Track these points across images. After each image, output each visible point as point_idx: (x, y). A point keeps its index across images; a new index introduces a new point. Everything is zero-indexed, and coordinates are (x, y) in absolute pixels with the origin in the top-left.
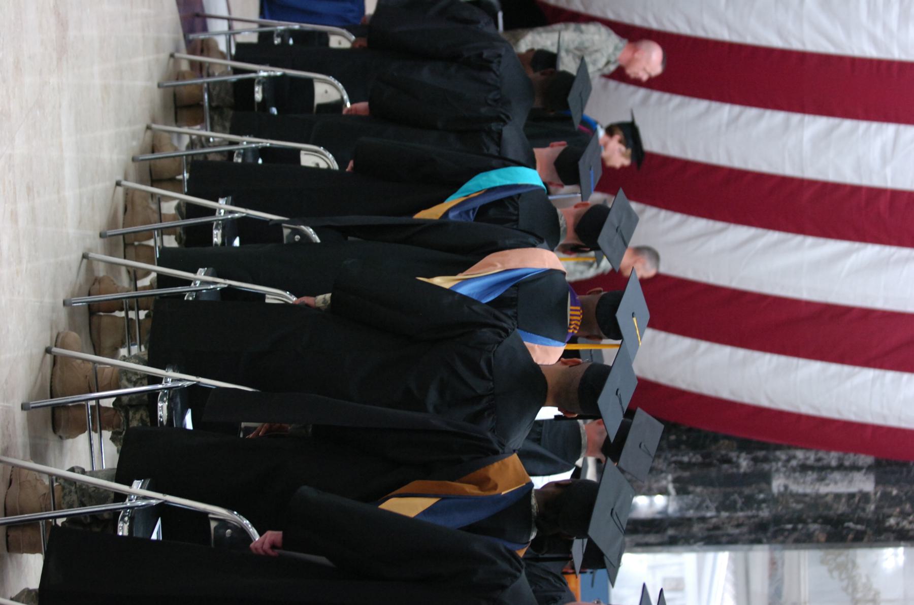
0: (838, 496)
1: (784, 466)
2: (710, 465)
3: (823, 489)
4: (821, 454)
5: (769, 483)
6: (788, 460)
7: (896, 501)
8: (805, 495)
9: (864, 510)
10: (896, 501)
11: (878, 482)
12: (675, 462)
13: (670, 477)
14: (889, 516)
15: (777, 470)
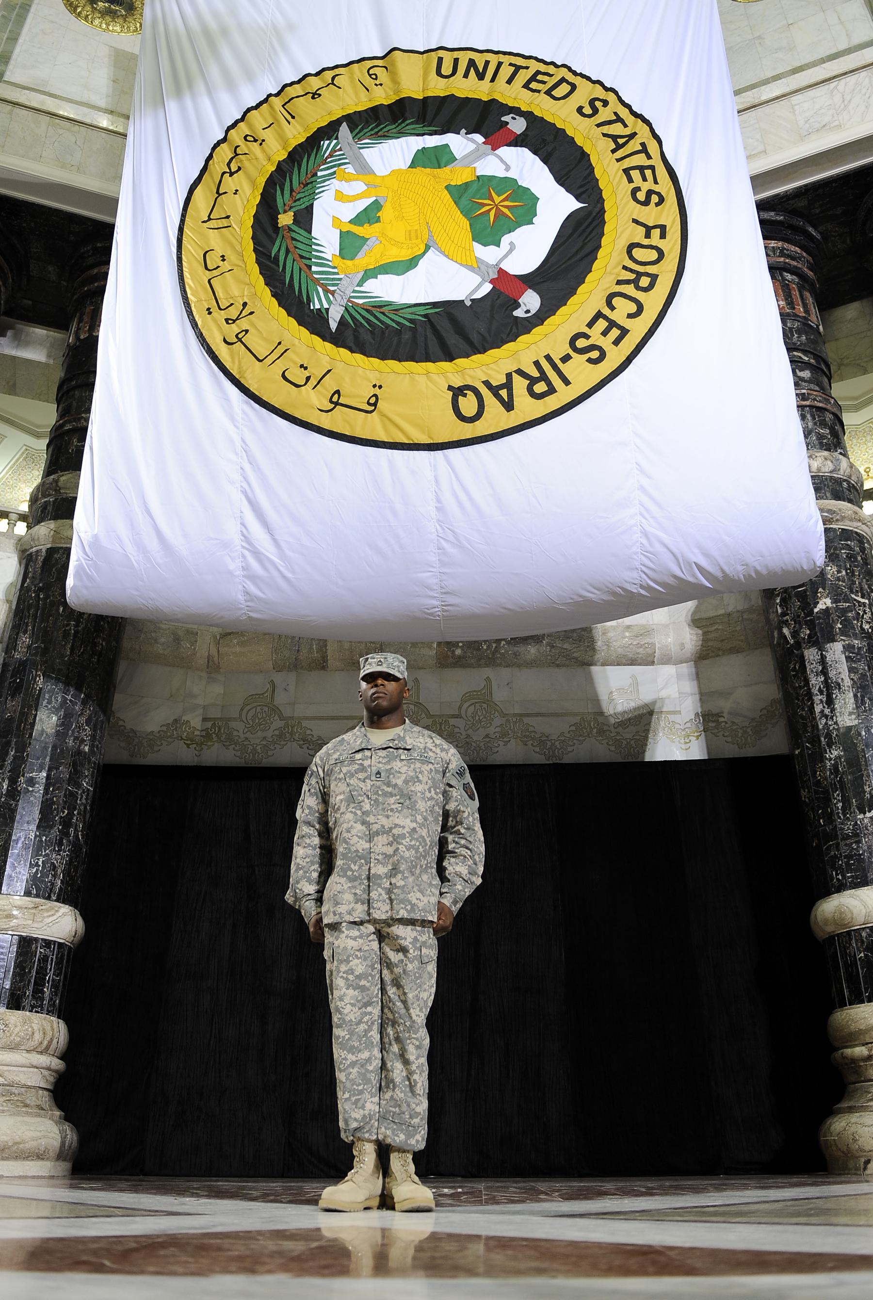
0: (851, 670)
1: (832, 718)
2: (841, 782)
3: (848, 682)
4: (815, 691)
5: (849, 728)
6: (826, 717)
7: (847, 623)
8: (855, 696)
9: (859, 648)
10: (847, 623)
11: (833, 640)
12: (844, 815)
13: (861, 816)
14: (862, 629)
15: (836, 723)
